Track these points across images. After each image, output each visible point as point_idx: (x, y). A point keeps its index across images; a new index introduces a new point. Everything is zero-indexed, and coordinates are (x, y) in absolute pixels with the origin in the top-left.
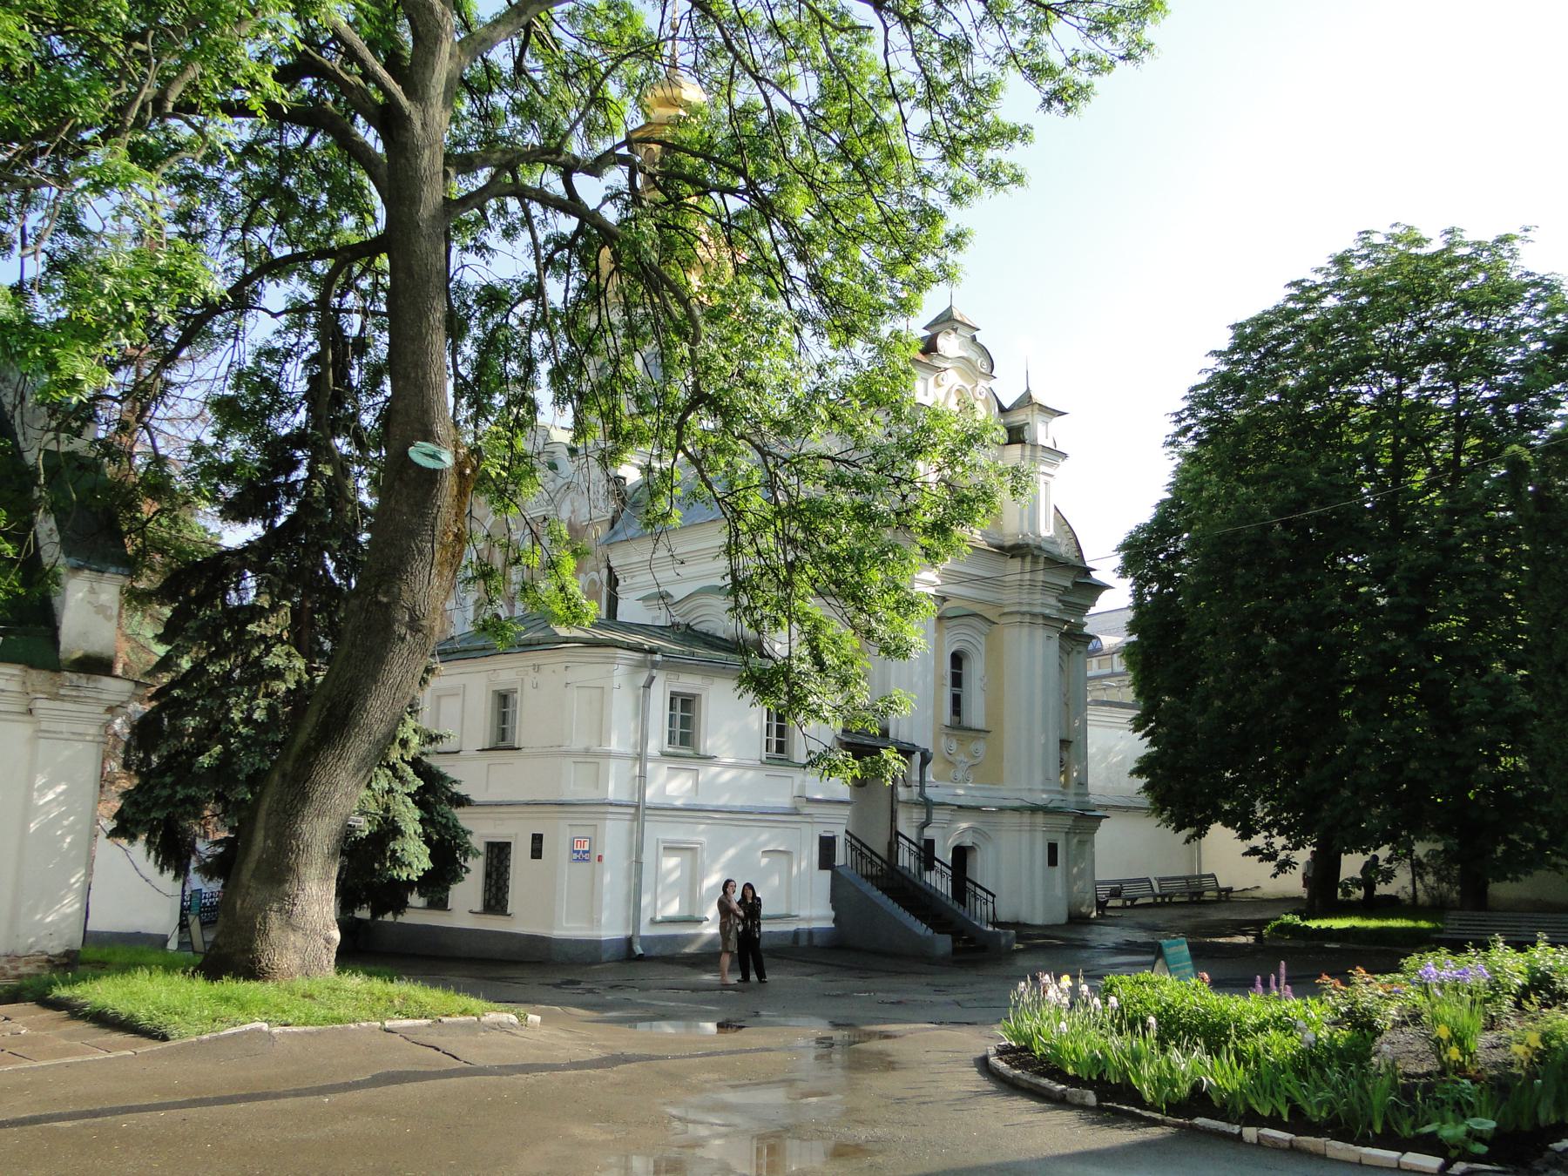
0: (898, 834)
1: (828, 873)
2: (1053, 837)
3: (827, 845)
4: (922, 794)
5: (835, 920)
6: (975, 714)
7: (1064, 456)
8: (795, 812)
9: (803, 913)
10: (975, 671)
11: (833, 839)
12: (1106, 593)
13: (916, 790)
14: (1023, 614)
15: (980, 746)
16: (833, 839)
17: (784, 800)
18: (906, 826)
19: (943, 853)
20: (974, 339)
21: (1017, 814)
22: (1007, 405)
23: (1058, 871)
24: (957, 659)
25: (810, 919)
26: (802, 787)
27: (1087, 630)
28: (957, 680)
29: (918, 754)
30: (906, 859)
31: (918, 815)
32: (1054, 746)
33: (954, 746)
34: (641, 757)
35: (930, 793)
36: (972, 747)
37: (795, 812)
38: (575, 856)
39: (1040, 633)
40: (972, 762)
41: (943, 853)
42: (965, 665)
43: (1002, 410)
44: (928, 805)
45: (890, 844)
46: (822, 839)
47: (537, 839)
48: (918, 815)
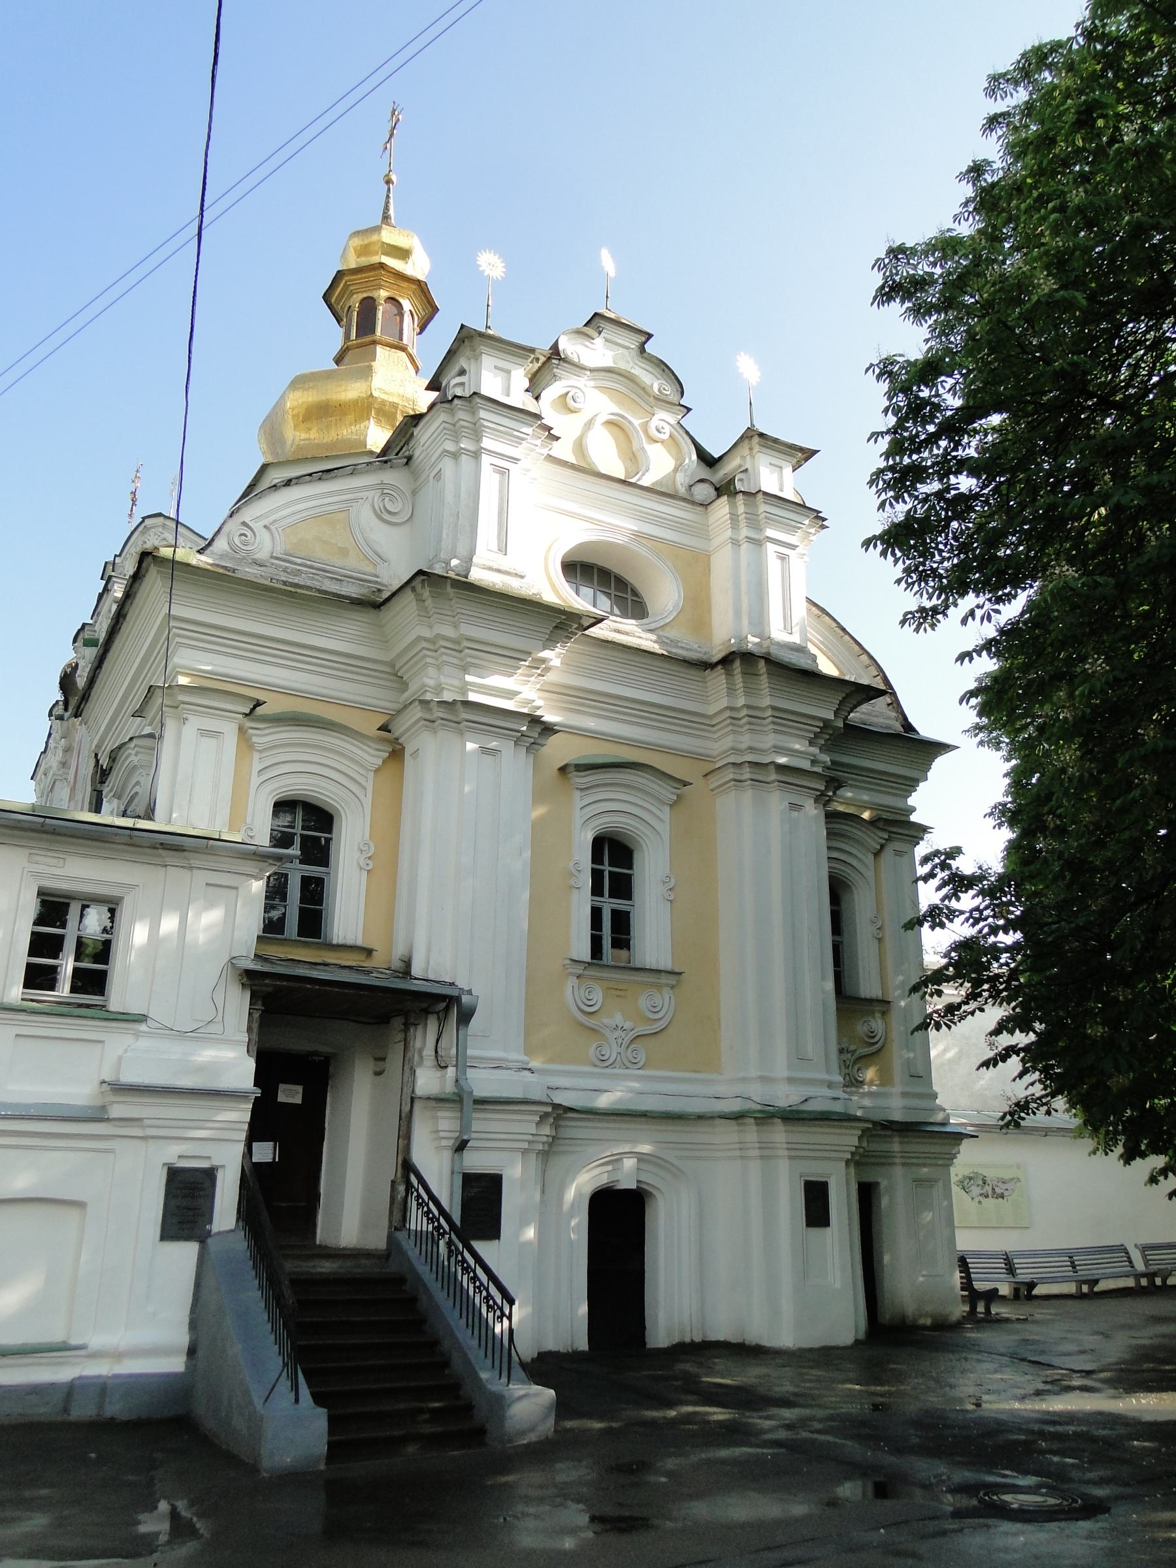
1: (186, 1253)
5: (192, 1352)
8: (98, 1115)
9: (96, 1341)
11: (210, 1175)
12: (940, 764)
15: (664, 1000)
16: (210, 1175)
17: (79, 1091)
21: (732, 1126)
25: (118, 1355)
27: (914, 818)
33: (598, 996)
36: (643, 1002)
37: (98, 1115)
39: (777, 800)
40: (643, 1029)
46: (174, 1174)
48: (447, 1122)
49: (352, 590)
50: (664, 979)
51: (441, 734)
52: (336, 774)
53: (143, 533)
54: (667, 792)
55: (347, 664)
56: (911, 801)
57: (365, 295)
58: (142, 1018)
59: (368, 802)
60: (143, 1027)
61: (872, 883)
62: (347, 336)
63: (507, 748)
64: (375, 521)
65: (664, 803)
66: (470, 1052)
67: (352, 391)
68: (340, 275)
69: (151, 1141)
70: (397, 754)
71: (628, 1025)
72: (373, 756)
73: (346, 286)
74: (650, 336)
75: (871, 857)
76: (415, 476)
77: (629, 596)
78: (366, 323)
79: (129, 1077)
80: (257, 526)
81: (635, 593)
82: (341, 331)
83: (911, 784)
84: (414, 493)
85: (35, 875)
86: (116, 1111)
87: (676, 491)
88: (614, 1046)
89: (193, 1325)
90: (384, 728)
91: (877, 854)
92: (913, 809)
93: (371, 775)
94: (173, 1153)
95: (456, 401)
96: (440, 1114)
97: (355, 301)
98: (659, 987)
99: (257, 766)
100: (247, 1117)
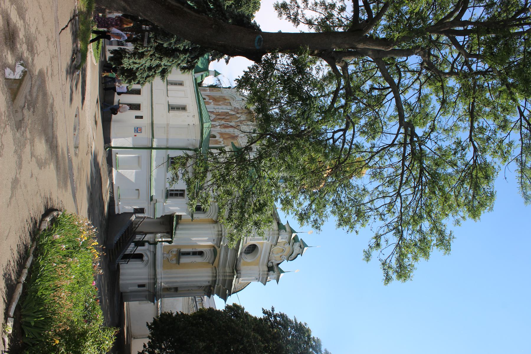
0: (146, 234)
1: (133, 211)
3: (141, 211)
5: (118, 214)
6: (184, 260)
7: (265, 284)
10: (198, 259)
12: (223, 301)
14: (216, 273)
15: (175, 262)
18: (148, 237)
19: (140, 250)
23: (136, 288)
24: (201, 253)
28: (195, 253)
30: (138, 237)
31: (152, 241)
32: (175, 285)
33: (174, 253)
35: (159, 244)
39: (210, 279)
41: (140, 250)
42: (199, 256)
43: (278, 264)
45: (142, 232)
47: (141, 117)
54: (211, 262)
59: (207, 218)
63: (215, 242)
72: (214, 218)
83: (218, 295)
86: (152, 202)
91: (204, 290)
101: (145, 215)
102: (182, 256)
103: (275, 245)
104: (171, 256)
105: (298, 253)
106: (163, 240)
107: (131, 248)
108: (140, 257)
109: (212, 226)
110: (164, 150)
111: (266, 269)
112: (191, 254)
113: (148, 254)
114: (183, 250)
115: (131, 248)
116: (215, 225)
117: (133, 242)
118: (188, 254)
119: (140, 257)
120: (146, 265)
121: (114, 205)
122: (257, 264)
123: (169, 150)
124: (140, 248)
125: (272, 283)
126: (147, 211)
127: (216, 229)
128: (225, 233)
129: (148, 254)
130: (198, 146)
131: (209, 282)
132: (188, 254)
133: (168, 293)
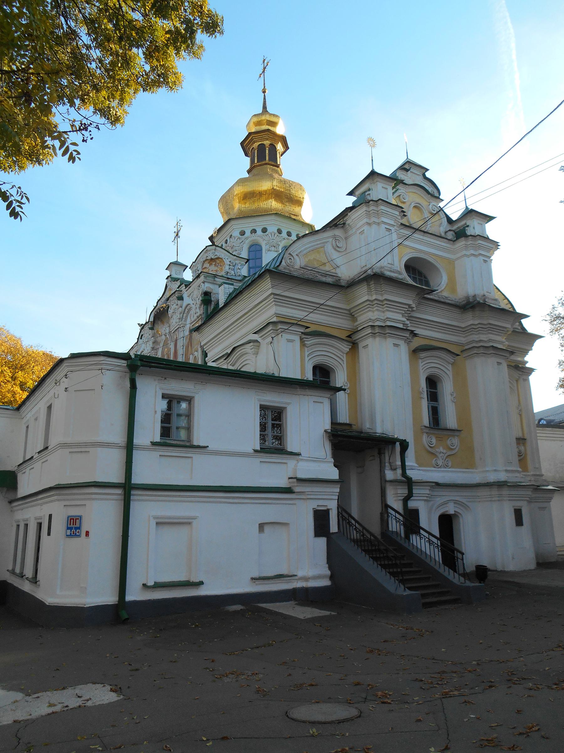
0: (387, 506)
1: (322, 541)
2: (518, 504)
3: (321, 519)
4: (404, 474)
5: (332, 578)
6: (450, 418)
8: (288, 490)
9: (300, 574)
10: (447, 389)
12: (538, 343)
13: (399, 471)
15: (455, 441)
18: (394, 500)
19: (429, 522)
20: (424, 175)
22: (454, 217)
25: (306, 579)
26: (295, 470)
27: (527, 365)
28: (433, 396)
29: (398, 444)
30: (395, 526)
31: (403, 491)
33: (434, 441)
34: (129, 447)
38: (69, 532)
41: (429, 522)
44: (409, 483)
45: (382, 514)
47: (50, 516)
49: (329, 280)
50: (457, 433)
51: (378, 339)
52: (334, 355)
53: (206, 253)
54: (450, 358)
55: (334, 311)
56: (526, 358)
57: (260, 143)
58: (299, 454)
59: (345, 366)
60: (300, 457)
61: (516, 392)
62: (252, 162)
63: (401, 343)
64: (333, 251)
65: (449, 363)
66: (407, 464)
67: (266, 186)
68: (250, 134)
69: (308, 501)
70: (354, 346)
71: (444, 451)
72: (346, 348)
73: (252, 139)
74: (427, 170)
75: (515, 382)
76: (346, 232)
77: (424, 279)
78: (261, 157)
79: (300, 476)
80: (294, 255)
81: (425, 277)
82: (248, 159)
84: (346, 238)
85: (259, 400)
86: (297, 489)
87: (441, 234)
88: (441, 459)
89: (330, 568)
90: (349, 336)
92: (527, 362)
93: (345, 355)
94: (314, 505)
95: (371, 202)
96: (398, 487)
97: (256, 145)
98: (453, 436)
99: (307, 353)
100: (338, 490)
101: (332, 505)
102: (442, 425)
103: (403, 214)
104: (441, 449)
105: (421, 177)
106: (399, 463)
107: (426, 546)
108: (447, 522)
109: (362, 353)
110: (137, 455)
111: (462, 242)
112: (434, 404)
113: (439, 500)
114: (426, 421)
115: (426, 546)
116: (361, 345)
117: (407, 537)
118: (435, 413)
119: (447, 522)
120: (466, 507)
121: (306, 590)
122: (451, 263)
123: (137, 441)
124: (424, 522)
125: (491, 230)
126: (321, 503)
127: (369, 341)
128: (377, 320)
129: (439, 500)
130: (124, 363)
131: (499, 363)
132: (435, 413)
133: (529, 458)
